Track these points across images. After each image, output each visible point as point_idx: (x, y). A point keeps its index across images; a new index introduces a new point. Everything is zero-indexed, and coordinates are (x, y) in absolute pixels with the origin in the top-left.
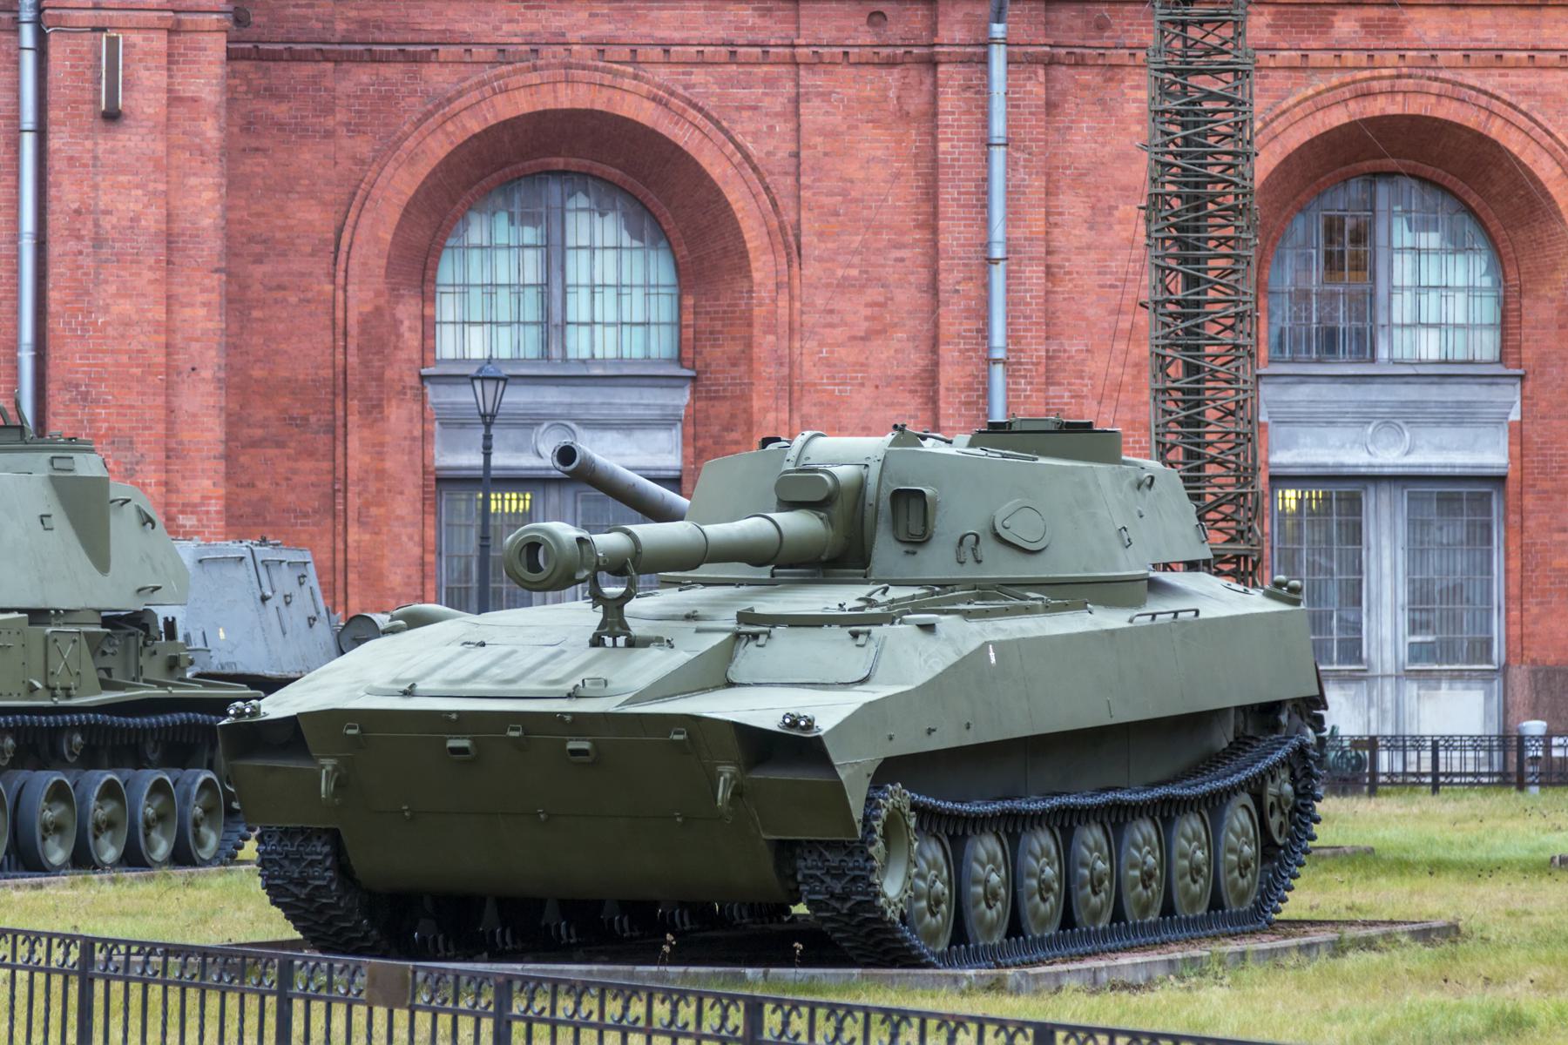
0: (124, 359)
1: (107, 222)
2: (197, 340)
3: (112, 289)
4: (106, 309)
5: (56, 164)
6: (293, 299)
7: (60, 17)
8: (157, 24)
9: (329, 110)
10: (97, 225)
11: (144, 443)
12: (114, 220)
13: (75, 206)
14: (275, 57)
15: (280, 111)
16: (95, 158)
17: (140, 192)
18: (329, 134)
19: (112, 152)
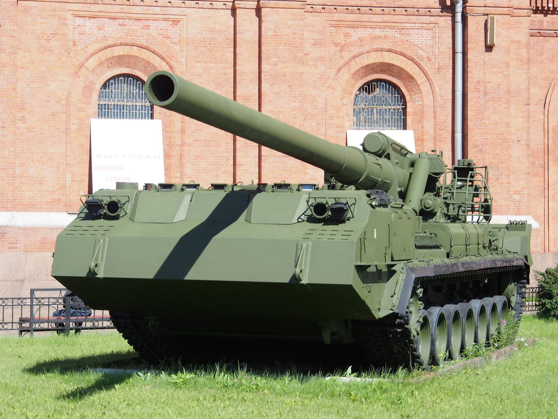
0: (495, 137)
1: (489, 86)
2: (520, 130)
3: (491, 111)
4: (488, 118)
5: (470, 64)
7: (472, 9)
8: (507, 13)
9: (542, 54)
10: (485, 87)
11: (502, 168)
12: (491, 85)
13: (477, 80)
16: (484, 62)
17: (501, 75)
18: (542, 62)
19: (491, 60)
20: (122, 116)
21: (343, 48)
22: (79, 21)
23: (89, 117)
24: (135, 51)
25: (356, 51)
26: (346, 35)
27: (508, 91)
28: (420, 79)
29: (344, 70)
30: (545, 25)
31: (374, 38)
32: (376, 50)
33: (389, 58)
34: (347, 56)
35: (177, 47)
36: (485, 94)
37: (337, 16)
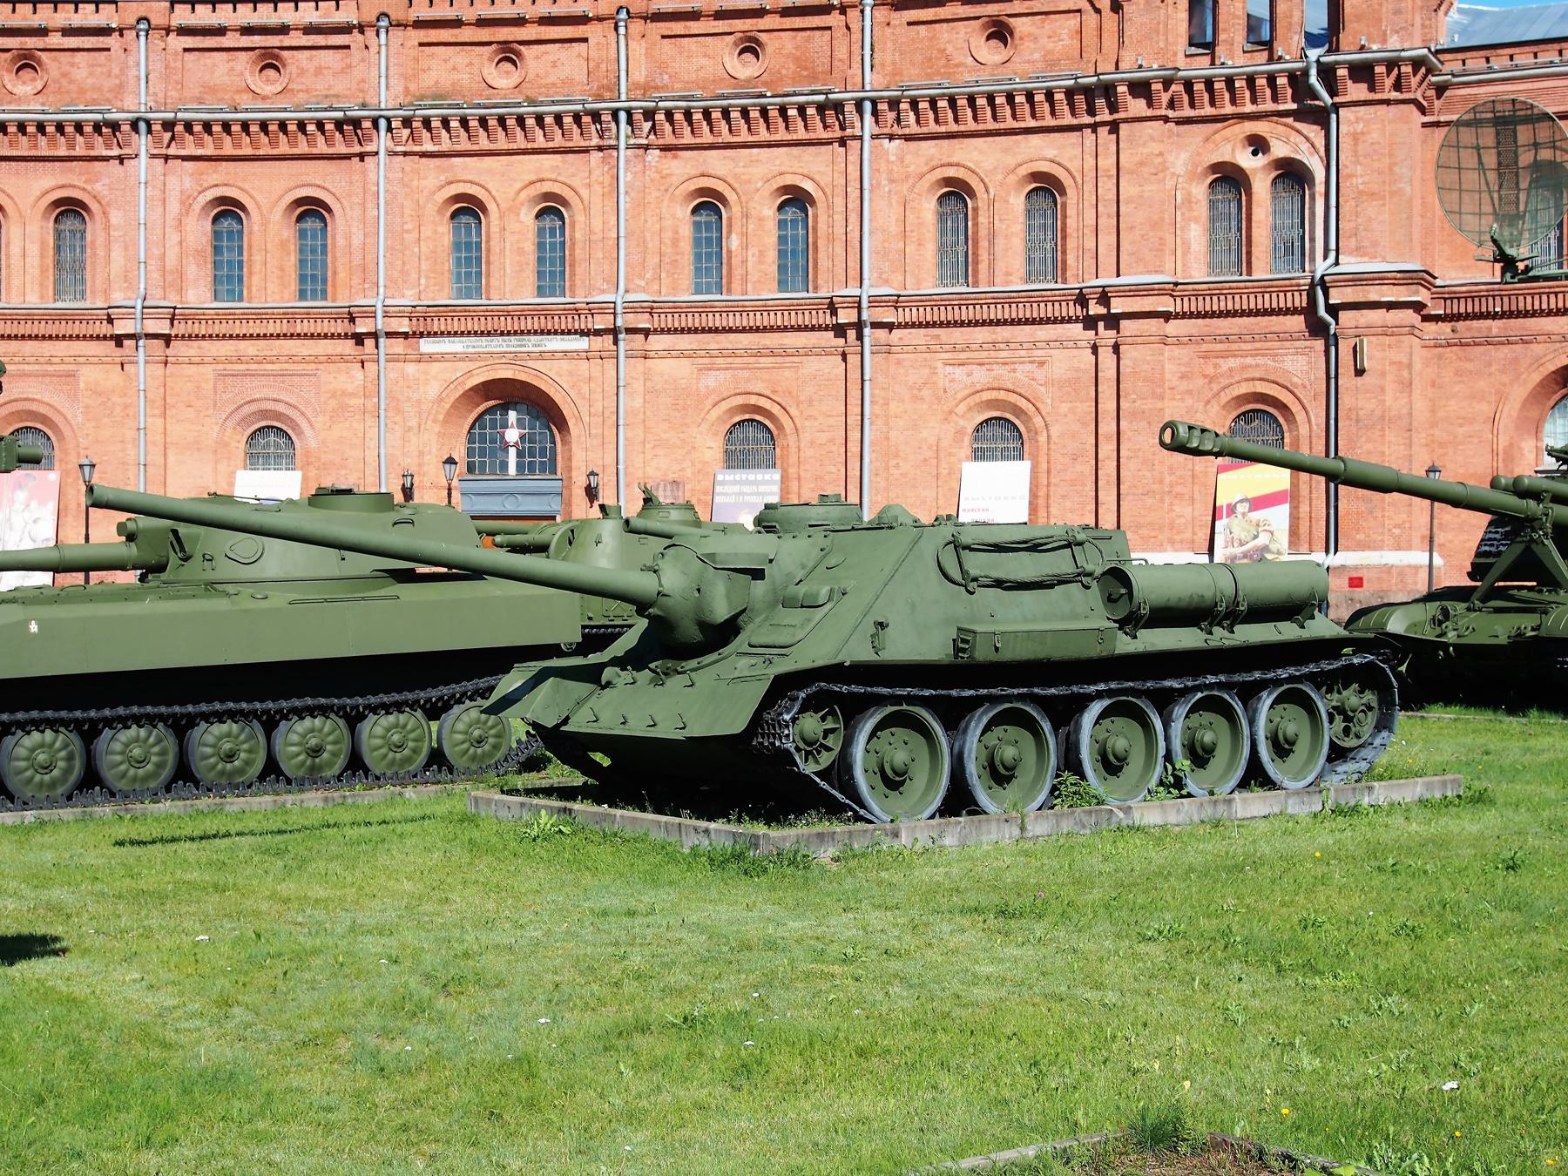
1: (1361, 413)
6: (1475, 441)
9: (1490, 365)
14: (1468, 345)
15: (1468, 366)
20: (995, 458)
21: (1211, 379)
22: (949, 369)
23: (960, 461)
24: (1002, 395)
25: (1225, 382)
26: (1216, 366)
27: (1383, 417)
28: (1295, 408)
29: (1214, 402)
30: (1495, 331)
31: (1245, 368)
32: (1247, 380)
33: (1261, 388)
34: (1216, 387)
35: (1042, 389)
36: (1358, 421)
37: (1205, 347)
